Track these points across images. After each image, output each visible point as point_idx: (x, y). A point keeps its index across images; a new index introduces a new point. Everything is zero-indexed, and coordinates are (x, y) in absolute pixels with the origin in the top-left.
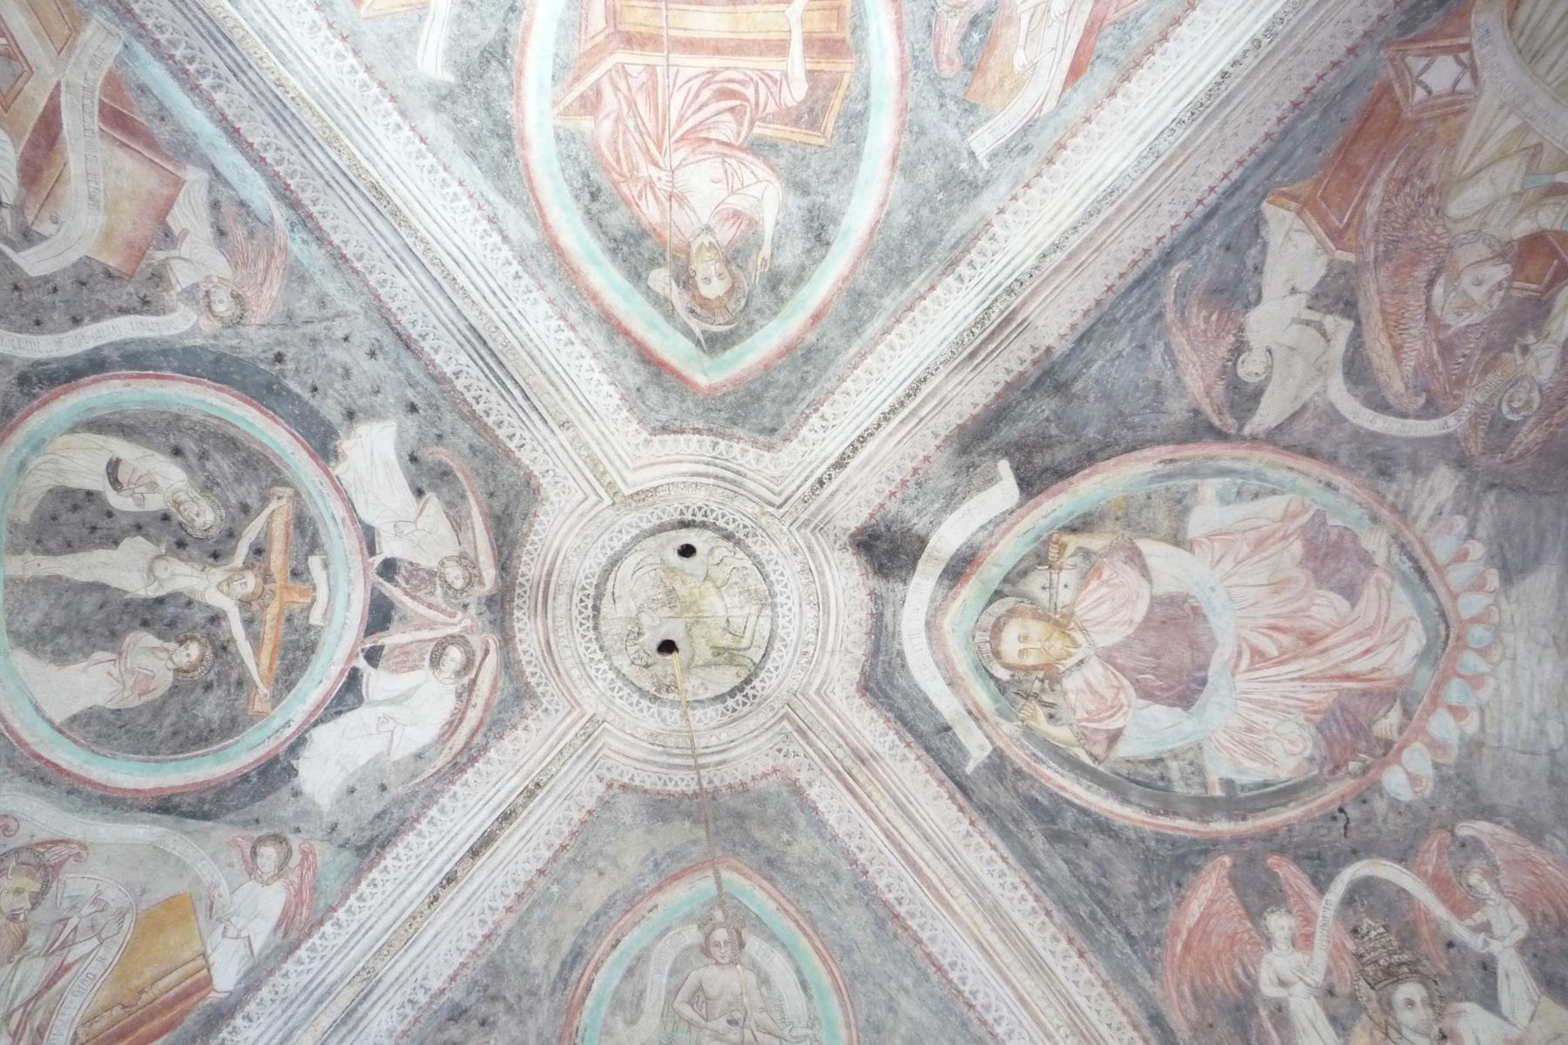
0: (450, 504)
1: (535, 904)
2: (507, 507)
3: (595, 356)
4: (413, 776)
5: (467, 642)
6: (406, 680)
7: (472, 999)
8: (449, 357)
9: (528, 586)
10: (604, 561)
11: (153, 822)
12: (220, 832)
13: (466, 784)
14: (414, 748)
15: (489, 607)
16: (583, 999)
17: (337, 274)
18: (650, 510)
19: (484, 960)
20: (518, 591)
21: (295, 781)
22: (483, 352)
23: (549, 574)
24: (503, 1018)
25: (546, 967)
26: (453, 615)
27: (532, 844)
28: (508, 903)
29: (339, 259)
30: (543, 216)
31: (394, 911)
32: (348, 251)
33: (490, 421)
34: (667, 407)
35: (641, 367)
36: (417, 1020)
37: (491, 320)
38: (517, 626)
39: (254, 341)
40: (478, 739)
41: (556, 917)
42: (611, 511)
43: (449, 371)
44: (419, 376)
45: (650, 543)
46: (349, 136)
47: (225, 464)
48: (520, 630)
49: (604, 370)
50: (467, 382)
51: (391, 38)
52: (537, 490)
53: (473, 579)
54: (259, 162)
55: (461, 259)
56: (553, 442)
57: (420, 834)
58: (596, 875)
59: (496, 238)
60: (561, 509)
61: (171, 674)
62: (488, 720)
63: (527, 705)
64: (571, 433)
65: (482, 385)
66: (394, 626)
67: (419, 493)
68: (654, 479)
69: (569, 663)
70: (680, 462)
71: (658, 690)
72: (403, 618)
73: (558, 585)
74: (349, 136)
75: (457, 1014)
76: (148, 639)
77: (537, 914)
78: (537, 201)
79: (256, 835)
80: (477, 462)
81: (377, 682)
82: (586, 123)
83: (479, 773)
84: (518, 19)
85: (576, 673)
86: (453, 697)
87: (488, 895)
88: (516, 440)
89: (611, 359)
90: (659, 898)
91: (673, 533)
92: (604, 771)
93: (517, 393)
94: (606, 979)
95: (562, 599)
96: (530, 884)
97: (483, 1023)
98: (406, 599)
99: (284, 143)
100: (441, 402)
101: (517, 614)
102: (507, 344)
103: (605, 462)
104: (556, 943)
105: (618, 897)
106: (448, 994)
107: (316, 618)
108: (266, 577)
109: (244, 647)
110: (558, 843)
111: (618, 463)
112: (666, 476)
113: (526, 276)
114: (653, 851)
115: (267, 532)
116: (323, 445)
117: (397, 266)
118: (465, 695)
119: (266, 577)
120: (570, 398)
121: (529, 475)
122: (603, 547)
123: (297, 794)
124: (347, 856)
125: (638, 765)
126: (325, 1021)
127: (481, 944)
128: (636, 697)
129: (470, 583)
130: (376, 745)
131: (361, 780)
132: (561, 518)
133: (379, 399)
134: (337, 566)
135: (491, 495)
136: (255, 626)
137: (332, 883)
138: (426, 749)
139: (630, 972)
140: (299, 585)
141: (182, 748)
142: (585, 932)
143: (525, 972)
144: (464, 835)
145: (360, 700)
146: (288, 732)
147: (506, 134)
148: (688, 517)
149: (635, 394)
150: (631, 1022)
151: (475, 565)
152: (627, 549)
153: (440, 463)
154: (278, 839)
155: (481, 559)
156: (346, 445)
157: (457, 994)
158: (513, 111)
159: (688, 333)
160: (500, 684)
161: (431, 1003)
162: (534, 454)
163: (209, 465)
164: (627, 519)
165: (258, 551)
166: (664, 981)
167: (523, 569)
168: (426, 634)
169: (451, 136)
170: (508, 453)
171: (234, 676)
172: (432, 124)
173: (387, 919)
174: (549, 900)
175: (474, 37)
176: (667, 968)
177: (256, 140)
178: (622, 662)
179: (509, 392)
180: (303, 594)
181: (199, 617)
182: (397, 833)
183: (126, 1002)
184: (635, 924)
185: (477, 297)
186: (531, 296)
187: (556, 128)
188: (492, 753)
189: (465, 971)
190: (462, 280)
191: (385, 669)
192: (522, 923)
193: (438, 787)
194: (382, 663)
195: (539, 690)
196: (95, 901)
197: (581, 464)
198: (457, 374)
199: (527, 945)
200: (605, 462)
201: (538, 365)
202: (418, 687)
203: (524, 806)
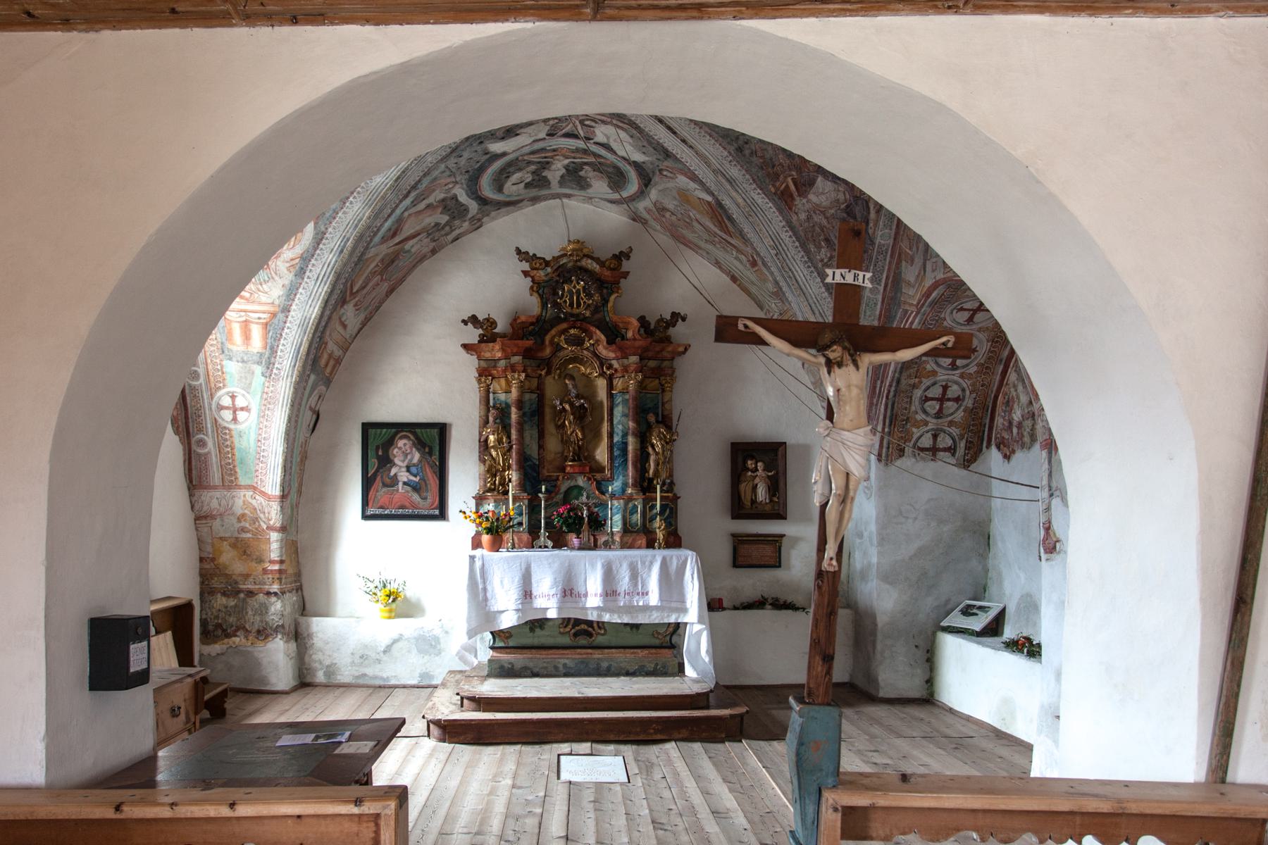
54: (397, 207)
126: (729, 187)
157: (732, 149)
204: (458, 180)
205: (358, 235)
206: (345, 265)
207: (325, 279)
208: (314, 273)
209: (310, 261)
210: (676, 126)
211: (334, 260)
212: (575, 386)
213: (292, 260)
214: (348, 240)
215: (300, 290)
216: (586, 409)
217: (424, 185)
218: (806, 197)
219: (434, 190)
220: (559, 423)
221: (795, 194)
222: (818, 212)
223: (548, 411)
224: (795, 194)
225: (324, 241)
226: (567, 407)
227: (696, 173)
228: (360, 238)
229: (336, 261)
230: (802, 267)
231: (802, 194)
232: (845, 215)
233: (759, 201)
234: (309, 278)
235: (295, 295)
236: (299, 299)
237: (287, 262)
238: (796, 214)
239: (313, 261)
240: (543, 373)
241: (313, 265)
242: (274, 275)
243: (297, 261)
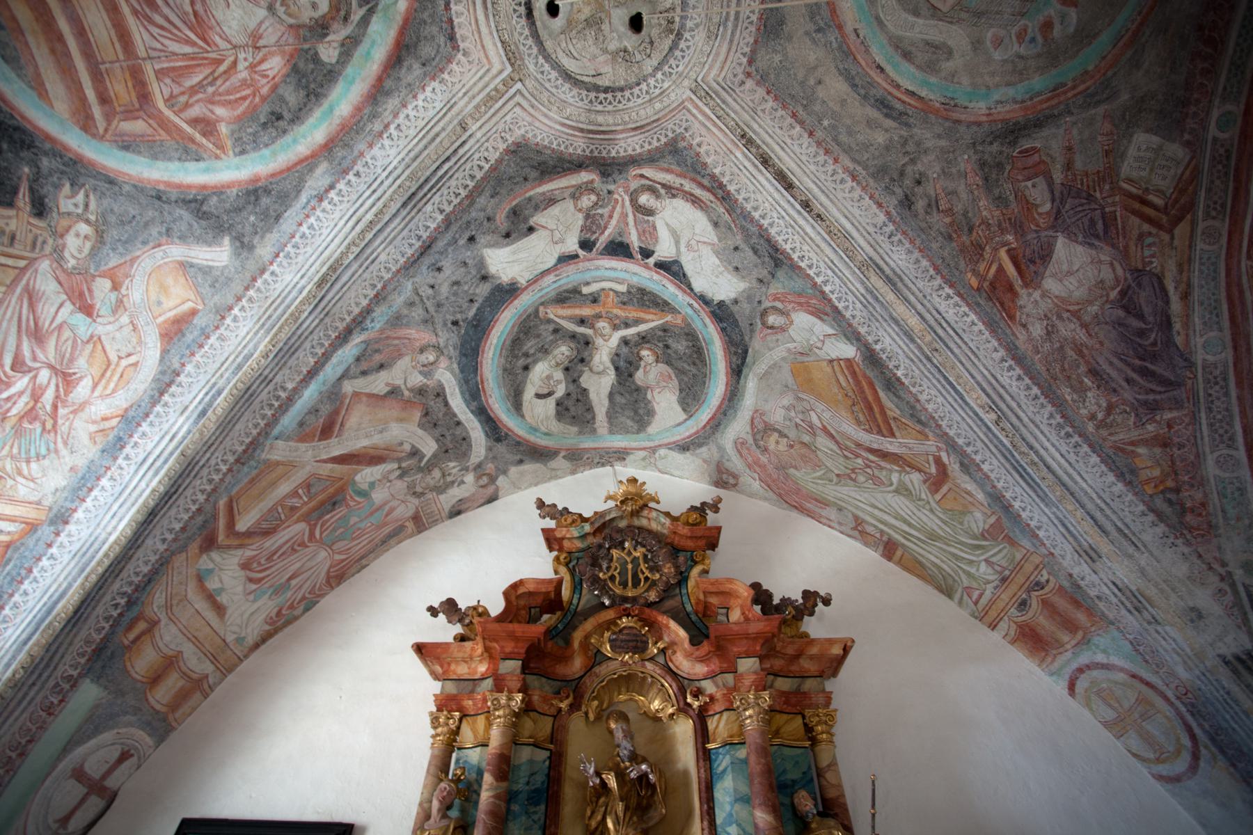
0: (537, 208)
1: (835, 140)
2: (533, 167)
3: (404, 106)
4: (730, 228)
5: (635, 190)
6: (663, 233)
7: (898, 191)
8: (430, 217)
9: (592, 147)
10: (567, 86)
11: (746, 378)
12: (756, 344)
13: (738, 191)
14: (710, 228)
15: (609, 175)
16: (920, 98)
17: (390, 298)
18: (521, 47)
19: (871, 181)
20: (596, 154)
21: (728, 302)
22: (421, 194)
23: (582, 130)
24: (919, 167)
25: (887, 131)
26: (616, 201)
27: (789, 141)
28: (831, 162)
29: (379, 298)
30: (306, 158)
31: (823, 245)
32: (372, 293)
33: (471, 184)
34: (433, 37)
35: (406, 64)
36: (904, 233)
37: (394, 192)
38: (622, 154)
39: (448, 338)
40: (706, 182)
41: (849, 122)
42: (527, 82)
43: (440, 217)
44: (448, 237)
45: (549, 44)
46: (288, 307)
47: (529, 345)
48: (625, 151)
49: (415, 97)
50: (446, 203)
51: (212, 286)
52: (518, 145)
53: (589, 188)
54: (326, 356)
55: (354, 219)
56: (479, 135)
57: (771, 225)
58: (820, 87)
59: (332, 194)
60: (530, 124)
61: (660, 365)
62: (692, 175)
63: (682, 144)
64: (469, 121)
65: (446, 192)
66: (625, 240)
67: (531, 230)
68: (495, 44)
69: (650, 111)
70: (477, 21)
71: (671, 31)
72: (620, 234)
73: (590, 123)
74: (288, 307)
75: (907, 202)
76: (639, 376)
77: (843, 138)
78: (296, 164)
79: (759, 325)
80: (503, 191)
81: (665, 250)
82: (223, 129)
83: (730, 181)
84: (165, 192)
85: (658, 106)
86: (674, 200)
87: (823, 177)
88: (483, 163)
89: (404, 92)
90: (849, 29)
91: (538, 24)
92: (737, 80)
93: (446, 167)
94: (906, 77)
95: (600, 119)
96: (819, 144)
97: (919, 183)
98: (607, 233)
99: (307, 345)
100: (465, 219)
101: (613, 154)
102: (410, 178)
103: (488, 90)
104: (870, 123)
105: (841, 67)
106: (891, 209)
107: (622, 288)
108: (598, 316)
109: (642, 328)
110: (789, 120)
111: (486, 79)
112: (491, 33)
113: (356, 168)
114: (807, 33)
115: (570, 319)
116: (509, 292)
117: (373, 262)
118: (674, 192)
119: (598, 316)
120: (441, 124)
121: (507, 151)
122: (557, 87)
123: (736, 302)
124: (780, 274)
125: (734, 49)
126: (891, 297)
127: (859, 183)
128: (678, 53)
129: (593, 190)
130: (706, 252)
131: (730, 263)
132: (537, 124)
133: (469, 262)
134: (588, 276)
135: (526, 179)
136: (629, 322)
137: (798, 284)
138: (711, 220)
139: (907, 56)
140: (602, 298)
141: (703, 362)
142: (865, 97)
143: (887, 148)
144: (776, 195)
145: (676, 262)
146: (695, 305)
147: (254, 192)
148: (522, 10)
149: (428, 68)
150: (950, 53)
151: (579, 187)
152: (557, 66)
153: (508, 217)
154: (764, 314)
155: (574, 183)
156: (505, 278)
157: (892, 202)
158: (235, 191)
159: (365, 22)
160: (666, 166)
161: (894, 222)
162: (491, 149)
163: (532, 351)
164: (532, 67)
165: (582, 322)
166: (921, 21)
167: (579, 151)
168: (631, 219)
169: (268, 235)
170: (493, 169)
171: (660, 333)
172: (264, 250)
173: (828, 251)
174: (834, 127)
175: (190, 225)
176: (911, 18)
177: (312, 361)
178: (649, 66)
179: (446, 172)
180: (607, 296)
181: (625, 350)
182: (768, 240)
183: (850, 403)
184: (867, 51)
185: (380, 204)
186: (370, 162)
187: (236, 155)
188: (717, 171)
189: (877, 196)
190: (369, 217)
191: (655, 245)
192: (847, 150)
193: (739, 211)
194: (651, 248)
195: (671, 135)
196: (788, 409)
197: (492, 111)
198: (442, 211)
199: (866, 146)
200: (488, 90)
201: (421, 153)
202: (667, 225)
203: (758, 147)
204: (442, 342)
205: (240, 385)
206: (209, 446)
207: (158, 464)
208: (140, 450)
209: (139, 425)
210: (793, 166)
211: (185, 429)
212: (629, 735)
213: (105, 419)
214: (219, 393)
215: (104, 482)
216: (653, 787)
217: (378, 326)
218: (1038, 286)
219: (401, 356)
220: (594, 824)
221: (1018, 283)
222: (1066, 315)
223: (569, 792)
224: (1018, 283)
225: (173, 389)
226: (612, 782)
227: (827, 289)
228: (245, 397)
229: (189, 432)
230: (1054, 438)
231: (1031, 281)
232: (1121, 313)
233: (950, 315)
234: (127, 458)
235: (91, 490)
236: (96, 499)
237: (94, 422)
238: (1024, 326)
239: (145, 427)
240: (564, 705)
241: (144, 434)
242: (60, 445)
243: (114, 422)
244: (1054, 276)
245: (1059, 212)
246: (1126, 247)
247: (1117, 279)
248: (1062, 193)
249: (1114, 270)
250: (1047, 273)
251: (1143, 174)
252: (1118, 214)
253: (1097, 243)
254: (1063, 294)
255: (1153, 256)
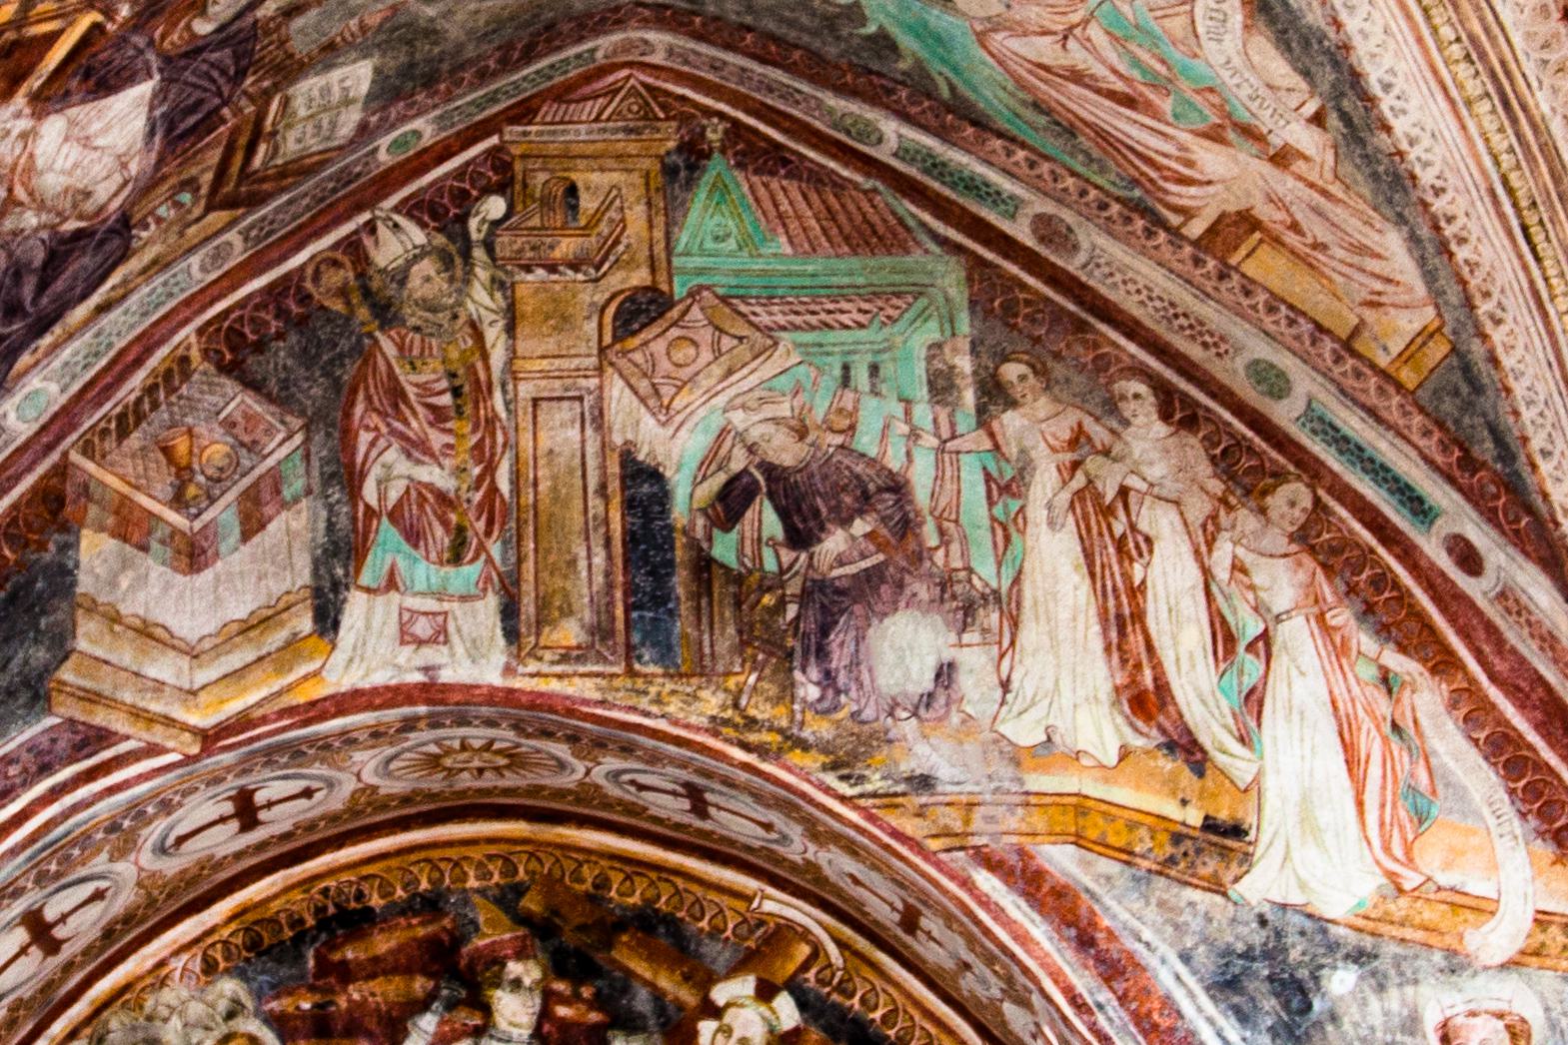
221: (35, 82)
224: (35, 82)
244: (72, 123)
245: (199, 51)
246: (164, 178)
247: (102, 208)
248: (240, 31)
249: (116, 194)
250: (73, 112)
251: (302, 112)
252: (222, 129)
253: (157, 139)
254: (40, 163)
255: (159, 220)
